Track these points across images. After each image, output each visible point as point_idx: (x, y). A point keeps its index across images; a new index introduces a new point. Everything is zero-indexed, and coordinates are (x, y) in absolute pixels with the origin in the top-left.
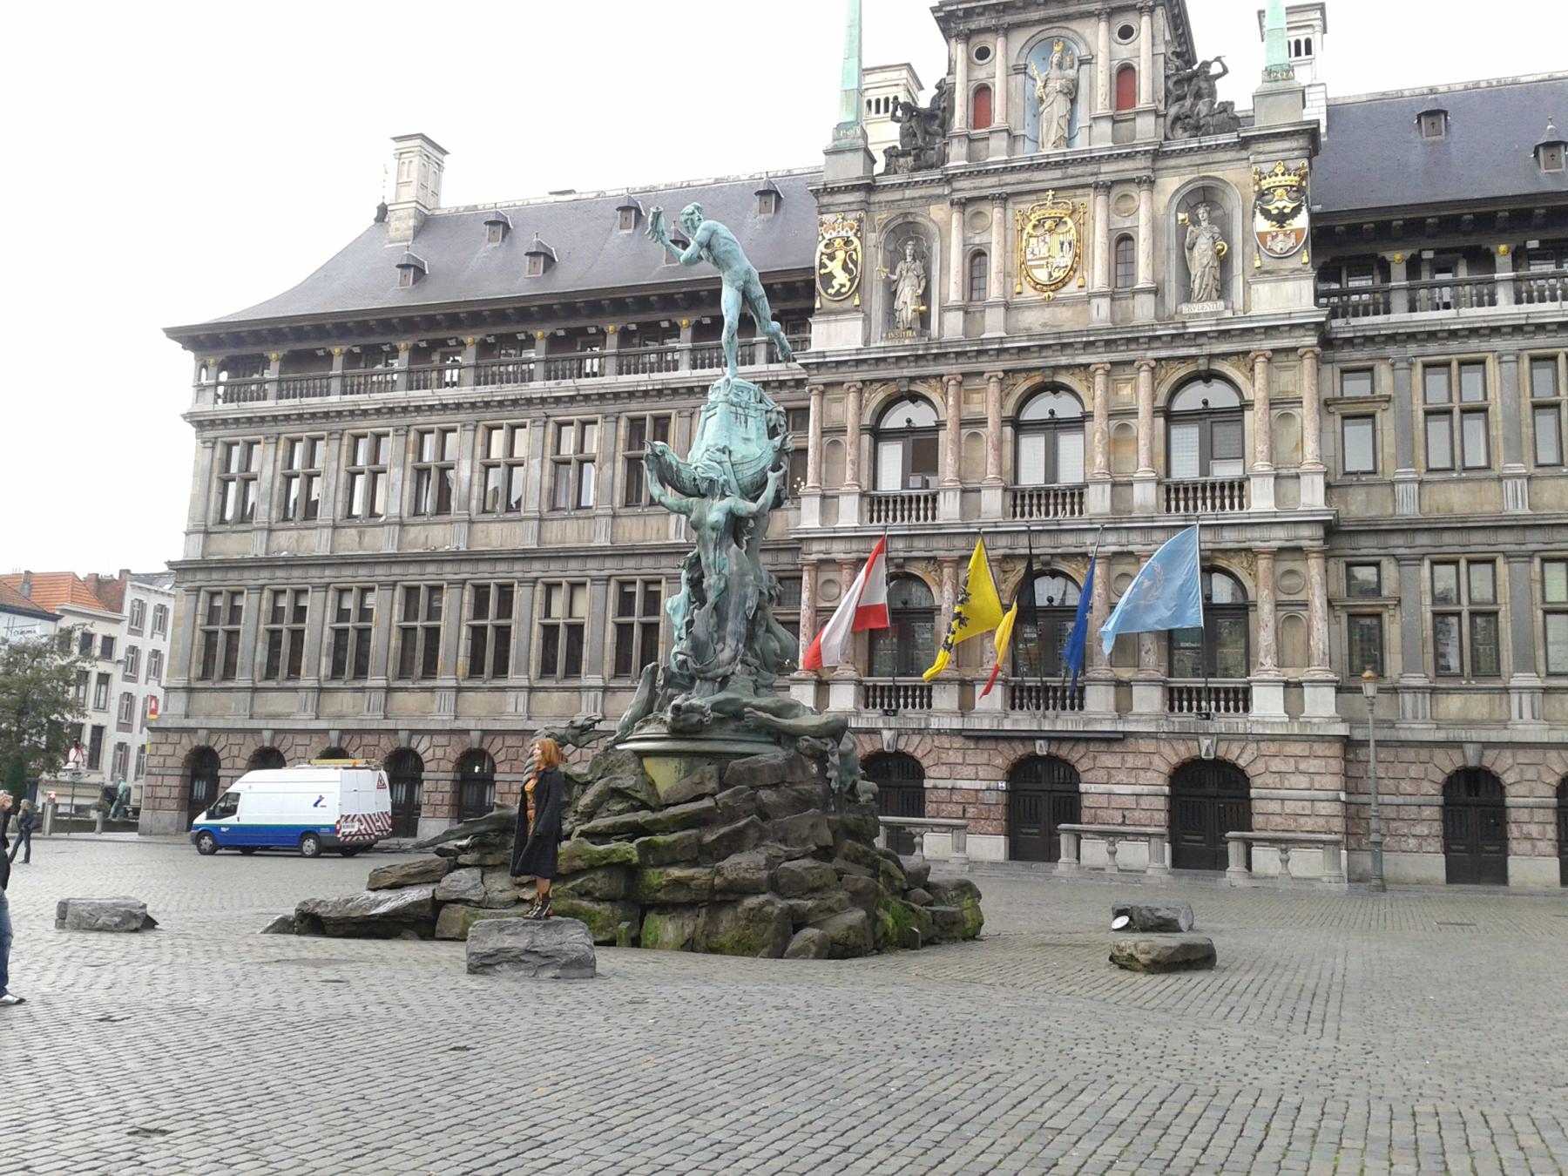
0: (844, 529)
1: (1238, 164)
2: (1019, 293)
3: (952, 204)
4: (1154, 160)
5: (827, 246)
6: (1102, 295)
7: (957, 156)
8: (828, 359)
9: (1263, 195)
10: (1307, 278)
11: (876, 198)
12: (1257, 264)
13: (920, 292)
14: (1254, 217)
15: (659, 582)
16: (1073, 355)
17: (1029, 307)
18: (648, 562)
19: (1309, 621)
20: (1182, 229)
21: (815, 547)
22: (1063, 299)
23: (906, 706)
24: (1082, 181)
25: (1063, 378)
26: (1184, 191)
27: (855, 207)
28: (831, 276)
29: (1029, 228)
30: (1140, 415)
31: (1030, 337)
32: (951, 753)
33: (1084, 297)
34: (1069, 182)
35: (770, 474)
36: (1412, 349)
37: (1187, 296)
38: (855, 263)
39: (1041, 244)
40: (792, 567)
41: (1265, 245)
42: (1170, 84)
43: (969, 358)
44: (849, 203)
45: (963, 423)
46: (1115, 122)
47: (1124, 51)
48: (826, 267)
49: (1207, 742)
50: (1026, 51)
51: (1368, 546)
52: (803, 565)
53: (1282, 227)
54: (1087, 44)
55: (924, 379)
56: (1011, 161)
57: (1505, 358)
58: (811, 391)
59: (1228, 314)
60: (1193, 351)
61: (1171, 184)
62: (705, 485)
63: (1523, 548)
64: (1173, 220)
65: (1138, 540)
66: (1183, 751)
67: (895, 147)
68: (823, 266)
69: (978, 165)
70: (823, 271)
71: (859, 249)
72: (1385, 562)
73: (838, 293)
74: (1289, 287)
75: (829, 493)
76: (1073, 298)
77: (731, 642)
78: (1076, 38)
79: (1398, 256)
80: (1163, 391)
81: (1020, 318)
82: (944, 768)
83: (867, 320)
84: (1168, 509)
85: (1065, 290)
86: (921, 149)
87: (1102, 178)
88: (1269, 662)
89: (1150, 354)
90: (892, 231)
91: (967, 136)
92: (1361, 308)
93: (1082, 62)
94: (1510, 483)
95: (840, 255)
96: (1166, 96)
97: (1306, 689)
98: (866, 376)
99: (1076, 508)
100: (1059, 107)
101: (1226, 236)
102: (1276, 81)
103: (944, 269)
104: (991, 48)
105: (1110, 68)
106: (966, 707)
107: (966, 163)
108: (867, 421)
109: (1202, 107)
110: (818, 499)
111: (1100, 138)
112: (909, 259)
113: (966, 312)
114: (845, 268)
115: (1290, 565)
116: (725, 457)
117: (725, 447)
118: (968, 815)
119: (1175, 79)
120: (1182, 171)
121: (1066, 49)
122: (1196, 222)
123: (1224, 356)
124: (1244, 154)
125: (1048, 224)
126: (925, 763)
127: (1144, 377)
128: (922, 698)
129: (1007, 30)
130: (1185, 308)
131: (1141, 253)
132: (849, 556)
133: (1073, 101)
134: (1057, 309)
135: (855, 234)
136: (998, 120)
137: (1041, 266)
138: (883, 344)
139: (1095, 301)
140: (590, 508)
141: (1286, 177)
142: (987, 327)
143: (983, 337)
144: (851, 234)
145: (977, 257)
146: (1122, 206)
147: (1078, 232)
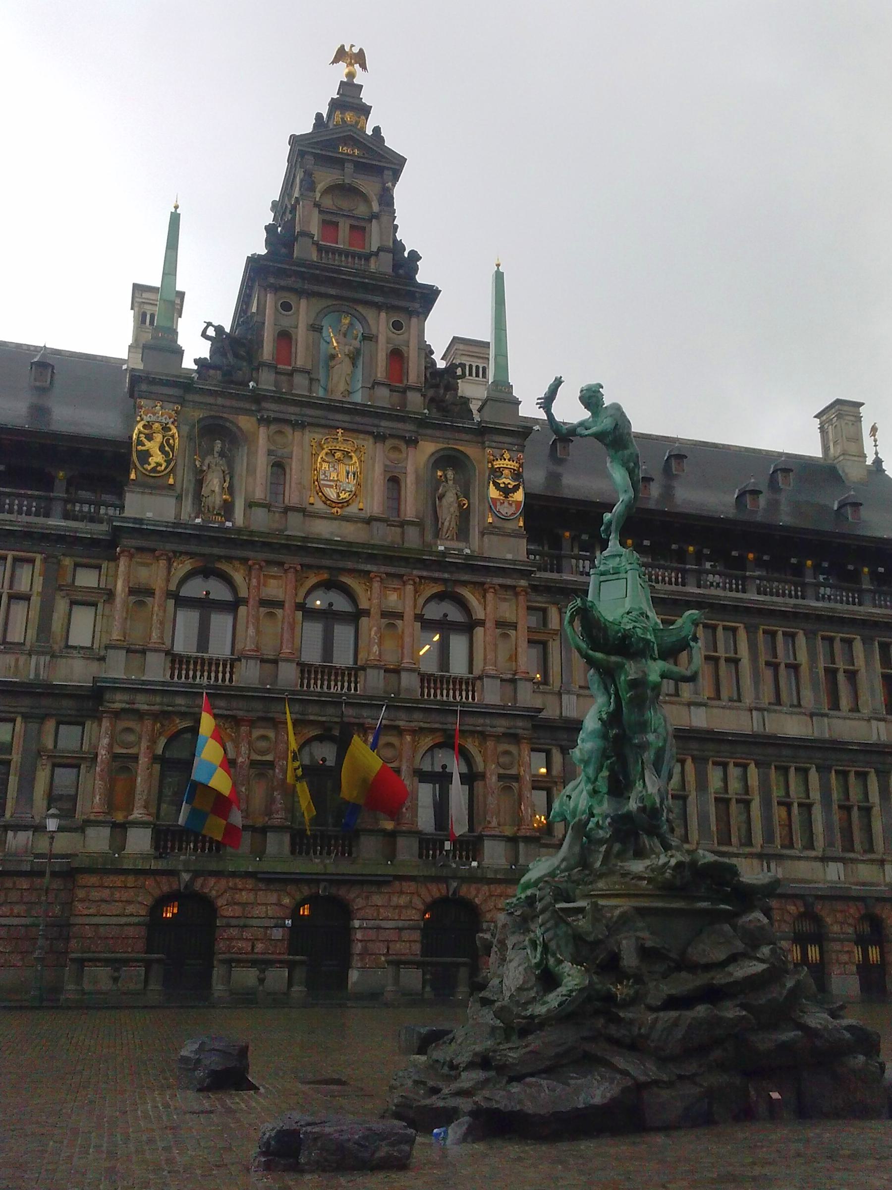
5: (144, 426)
8: (145, 527)
11: (189, 397)
12: (490, 520)
14: (488, 489)
16: (358, 562)
21: (119, 696)
29: (322, 454)
30: (405, 618)
31: (328, 541)
32: (244, 893)
34: (355, 427)
38: (172, 448)
39: (332, 469)
46: (391, 390)
48: (144, 445)
49: (455, 884)
53: (506, 497)
58: (122, 552)
60: (446, 576)
61: (428, 448)
62: (641, 645)
66: (436, 891)
67: (205, 359)
68: (142, 444)
70: (140, 448)
73: (154, 470)
79: (567, 534)
80: (421, 601)
87: (381, 430)
89: (415, 572)
95: (158, 438)
99: (353, 685)
103: (251, 470)
105: (387, 348)
106: (260, 852)
108: (173, 587)
112: (216, 455)
114: (161, 448)
118: (256, 951)
125: (338, 455)
126: (220, 902)
132: (153, 708)
133: (354, 365)
135: (173, 423)
137: (331, 487)
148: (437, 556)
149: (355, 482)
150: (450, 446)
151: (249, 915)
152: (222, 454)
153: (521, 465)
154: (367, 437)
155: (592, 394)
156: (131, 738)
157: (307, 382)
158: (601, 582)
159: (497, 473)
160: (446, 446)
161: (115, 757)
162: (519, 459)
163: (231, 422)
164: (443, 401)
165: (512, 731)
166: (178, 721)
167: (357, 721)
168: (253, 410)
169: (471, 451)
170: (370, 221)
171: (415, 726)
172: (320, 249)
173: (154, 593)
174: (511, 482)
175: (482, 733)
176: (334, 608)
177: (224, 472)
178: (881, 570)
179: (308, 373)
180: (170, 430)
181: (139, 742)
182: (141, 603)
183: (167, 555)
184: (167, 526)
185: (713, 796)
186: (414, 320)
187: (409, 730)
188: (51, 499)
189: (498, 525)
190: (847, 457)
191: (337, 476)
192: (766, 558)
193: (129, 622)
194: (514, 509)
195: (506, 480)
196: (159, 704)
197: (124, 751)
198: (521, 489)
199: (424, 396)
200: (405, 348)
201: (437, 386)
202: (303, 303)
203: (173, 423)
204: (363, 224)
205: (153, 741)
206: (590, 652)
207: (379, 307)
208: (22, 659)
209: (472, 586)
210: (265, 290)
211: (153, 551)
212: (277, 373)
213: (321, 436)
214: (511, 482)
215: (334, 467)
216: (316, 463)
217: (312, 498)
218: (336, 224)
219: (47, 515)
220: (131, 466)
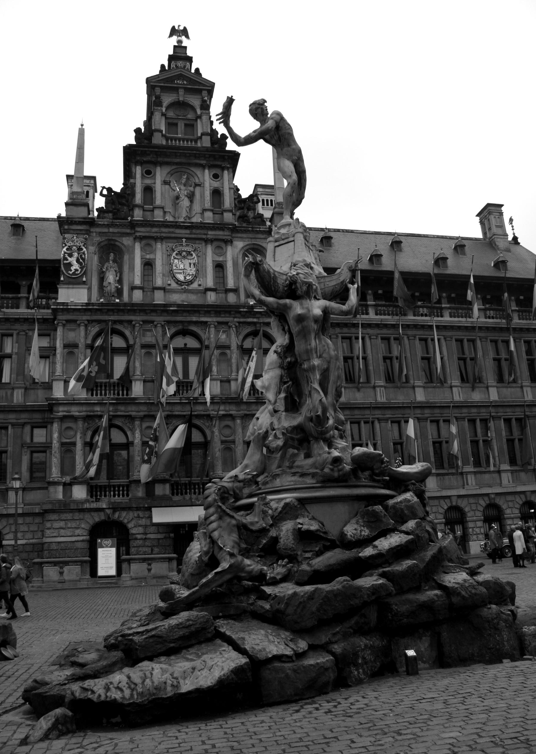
2: (169, 285)
4: (232, 233)
5: (67, 249)
7: (138, 214)
8: (69, 307)
13: (118, 278)
16: (199, 317)
21: (61, 408)
23: (101, 496)
24: (200, 236)
25: (194, 328)
26: (245, 248)
27: (84, 232)
28: (70, 265)
29: (174, 254)
30: (232, 348)
31: (179, 305)
32: (144, 520)
33: (202, 290)
34: (193, 236)
35: (350, 286)
36: (338, 330)
38: (84, 259)
39: (180, 263)
40: (41, 421)
42: (236, 202)
43: (147, 314)
45: (143, 346)
46: (213, 214)
47: (216, 184)
52: (53, 418)
55: (121, 322)
57: (372, 337)
60: (255, 320)
61: (239, 244)
62: (305, 288)
63: (385, 416)
65: (234, 408)
67: (102, 208)
70: (65, 262)
71: (86, 252)
73: (74, 274)
76: (196, 290)
78: (193, 174)
80: (241, 337)
81: (170, 296)
82: (140, 528)
83: (90, 289)
86: (118, 210)
87: (208, 236)
89: (235, 320)
90: (102, 247)
93: (196, 185)
95: (76, 255)
98: (89, 318)
100: (185, 202)
103: (132, 268)
105: (210, 190)
108: (89, 342)
111: (209, 218)
112: (111, 262)
113: (143, 291)
114: (78, 261)
121: (188, 179)
126: (130, 526)
128: (123, 491)
129: (162, 164)
131: (228, 273)
132: (81, 414)
133: (191, 201)
134: (189, 295)
136: (158, 202)
137: (180, 273)
139: (209, 293)
142: (155, 299)
145: (148, 265)
146: (217, 251)
147: (198, 260)
151: (148, 532)
152: (114, 261)
154: (201, 242)
155: (257, 106)
156: (72, 433)
158: (275, 247)
161: (63, 444)
164: (246, 216)
166: (97, 421)
167: (205, 413)
170: (196, 120)
172: (167, 139)
176: (188, 346)
177: (116, 271)
178: (522, 297)
179: (163, 208)
180: (82, 249)
181: (75, 435)
182: (71, 353)
183: (84, 323)
184: (82, 306)
185: (431, 440)
186: (226, 172)
187: (239, 417)
188: (19, 298)
190: (495, 236)
192: (453, 295)
196: (84, 411)
197: (68, 441)
199: (234, 215)
200: (221, 189)
201: (242, 208)
202: (158, 169)
203: (84, 246)
204: (192, 122)
205: (84, 434)
206: (263, 298)
207: (203, 167)
208: (9, 392)
211: (75, 321)
212: (144, 210)
213: (173, 244)
215: (181, 261)
216: (170, 260)
218: (176, 125)
219: (18, 308)
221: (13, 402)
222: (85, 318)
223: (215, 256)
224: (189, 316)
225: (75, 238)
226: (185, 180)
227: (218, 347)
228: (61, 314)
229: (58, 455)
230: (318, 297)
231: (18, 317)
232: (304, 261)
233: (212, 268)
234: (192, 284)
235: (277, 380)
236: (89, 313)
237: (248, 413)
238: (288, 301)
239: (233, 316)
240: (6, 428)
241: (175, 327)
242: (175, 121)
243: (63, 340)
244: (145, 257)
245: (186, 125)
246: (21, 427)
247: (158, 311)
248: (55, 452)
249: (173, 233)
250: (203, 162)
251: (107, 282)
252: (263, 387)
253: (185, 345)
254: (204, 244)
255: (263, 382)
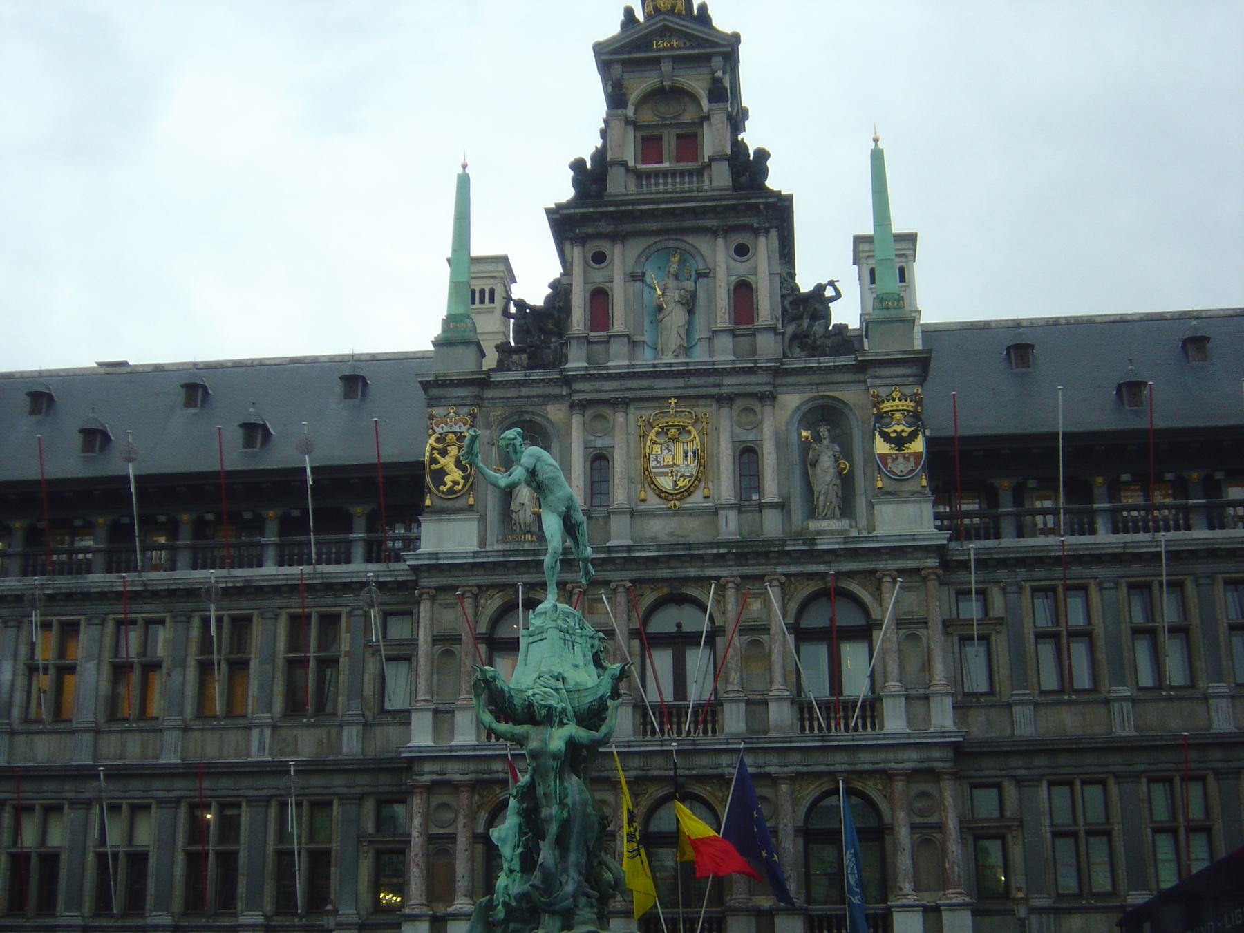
0: (462, 747)
1: (853, 387)
2: (644, 500)
3: (573, 406)
5: (437, 440)
6: (731, 507)
8: (441, 562)
9: (882, 417)
10: (925, 501)
11: (488, 394)
12: (879, 484)
15: (238, 806)
16: (703, 567)
17: (655, 516)
18: (225, 783)
19: (944, 843)
20: (805, 447)
21: (428, 767)
22: (686, 509)
24: (704, 391)
26: (804, 408)
27: (468, 401)
28: (442, 473)
29: (652, 435)
30: (772, 632)
31: (659, 547)
33: (709, 508)
34: (691, 392)
35: (610, 703)
36: (1022, 573)
37: (812, 512)
39: (665, 452)
40: (394, 789)
41: (886, 465)
42: (787, 303)
44: (462, 398)
47: (741, 268)
50: (643, 259)
51: (990, 768)
52: (414, 787)
54: (704, 259)
56: (634, 366)
57: (1106, 585)
58: (421, 595)
59: (854, 533)
60: (822, 568)
61: (791, 401)
63: (1131, 768)
64: (794, 436)
68: (434, 461)
69: (599, 368)
70: (434, 467)
72: (1006, 784)
73: (451, 491)
74: (909, 509)
75: (442, 707)
77: (573, 873)
78: (693, 251)
80: (793, 606)
83: (482, 520)
84: (803, 729)
85: (690, 500)
86: (537, 347)
87: (724, 390)
88: (907, 887)
89: (780, 569)
91: (586, 338)
92: (973, 532)
93: (700, 275)
94: (1116, 705)
95: (453, 451)
96: (783, 314)
97: (943, 913)
100: (676, 317)
101: (847, 453)
102: (888, 308)
104: (607, 253)
105: (729, 285)
107: (586, 365)
108: (482, 629)
109: (818, 328)
110: (429, 715)
111: (724, 352)
114: (458, 464)
115: (922, 787)
116: (560, 685)
117: (560, 673)
119: (791, 299)
120: (802, 389)
121: (682, 262)
122: (818, 439)
123: (850, 575)
124: (861, 377)
125: (673, 431)
127: (773, 594)
130: (813, 526)
133: (691, 312)
136: (619, 324)
137: (665, 474)
138: (500, 547)
140: (156, 719)
141: (903, 402)
143: (608, 544)
144: (464, 429)
145: (599, 461)
146: (744, 419)
147: (702, 444)
148: (804, 544)
149: (696, 462)
150: (821, 394)
153: (919, 403)
154: (709, 402)
156: (449, 816)
157: (625, 349)
158: (529, 643)
159: (882, 418)
160: (816, 394)
161: (431, 839)
162: (916, 394)
163: (538, 415)
165: (926, 765)
166: (498, 791)
167: (715, 771)
168: (565, 396)
169: (849, 395)
171: (793, 772)
173: (460, 639)
174: (906, 429)
175: (884, 772)
176: (685, 629)
179: (628, 336)
181: (455, 820)
183: (471, 591)
184: (466, 558)
187: (784, 778)
188: (351, 542)
189: (890, 489)
191: (673, 459)
193: (435, 676)
194: (912, 464)
195: (899, 427)
196: (472, 772)
197: (441, 831)
198: (920, 437)
200: (753, 278)
202: (618, 247)
204: (689, 130)
205: (472, 817)
207: (713, 232)
208: (334, 732)
209: (862, 576)
210: (572, 243)
213: (651, 411)
214: (906, 429)
215: (667, 448)
216: (644, 448)
217: (643, 493)
218: (660, 138)
220: (426, 491)
221: (340, 753)
222: (473, 581)
223: (738, 430)
224: (681, 568)
225: (452, 414)
226: (675, 266)
227: (743, 631)
228: (426, 575)
229: (420, 860)
230: (565, 721)
231: (349, 580)
232: (551, 671)
233: (731, 459)
234: (689, 495)
235: (516, 830)
236: (482, 572)
237: (805, 769)
238: (525, 728)
239: (775, 561)
240: (330, 804)
241: (653, 590)
242: (657, 133)
243: (432, 629)
244: (593, 444)
245: (679, 137)
246: (357, 802)
247: (618, 561)
248: (416, 855)
249: (651, 388)
250: (712, 223)
251: (517, 504)
252: (499, 839)
253: (679, 625)
254: (714, 407)
255: (499, 833)
